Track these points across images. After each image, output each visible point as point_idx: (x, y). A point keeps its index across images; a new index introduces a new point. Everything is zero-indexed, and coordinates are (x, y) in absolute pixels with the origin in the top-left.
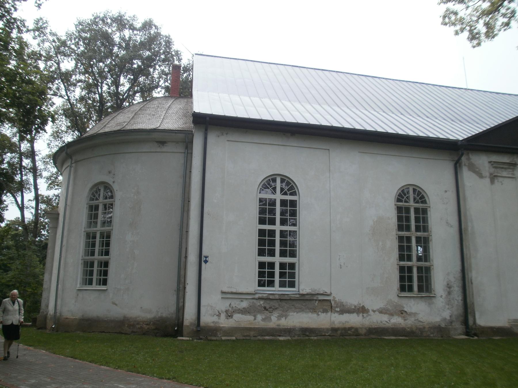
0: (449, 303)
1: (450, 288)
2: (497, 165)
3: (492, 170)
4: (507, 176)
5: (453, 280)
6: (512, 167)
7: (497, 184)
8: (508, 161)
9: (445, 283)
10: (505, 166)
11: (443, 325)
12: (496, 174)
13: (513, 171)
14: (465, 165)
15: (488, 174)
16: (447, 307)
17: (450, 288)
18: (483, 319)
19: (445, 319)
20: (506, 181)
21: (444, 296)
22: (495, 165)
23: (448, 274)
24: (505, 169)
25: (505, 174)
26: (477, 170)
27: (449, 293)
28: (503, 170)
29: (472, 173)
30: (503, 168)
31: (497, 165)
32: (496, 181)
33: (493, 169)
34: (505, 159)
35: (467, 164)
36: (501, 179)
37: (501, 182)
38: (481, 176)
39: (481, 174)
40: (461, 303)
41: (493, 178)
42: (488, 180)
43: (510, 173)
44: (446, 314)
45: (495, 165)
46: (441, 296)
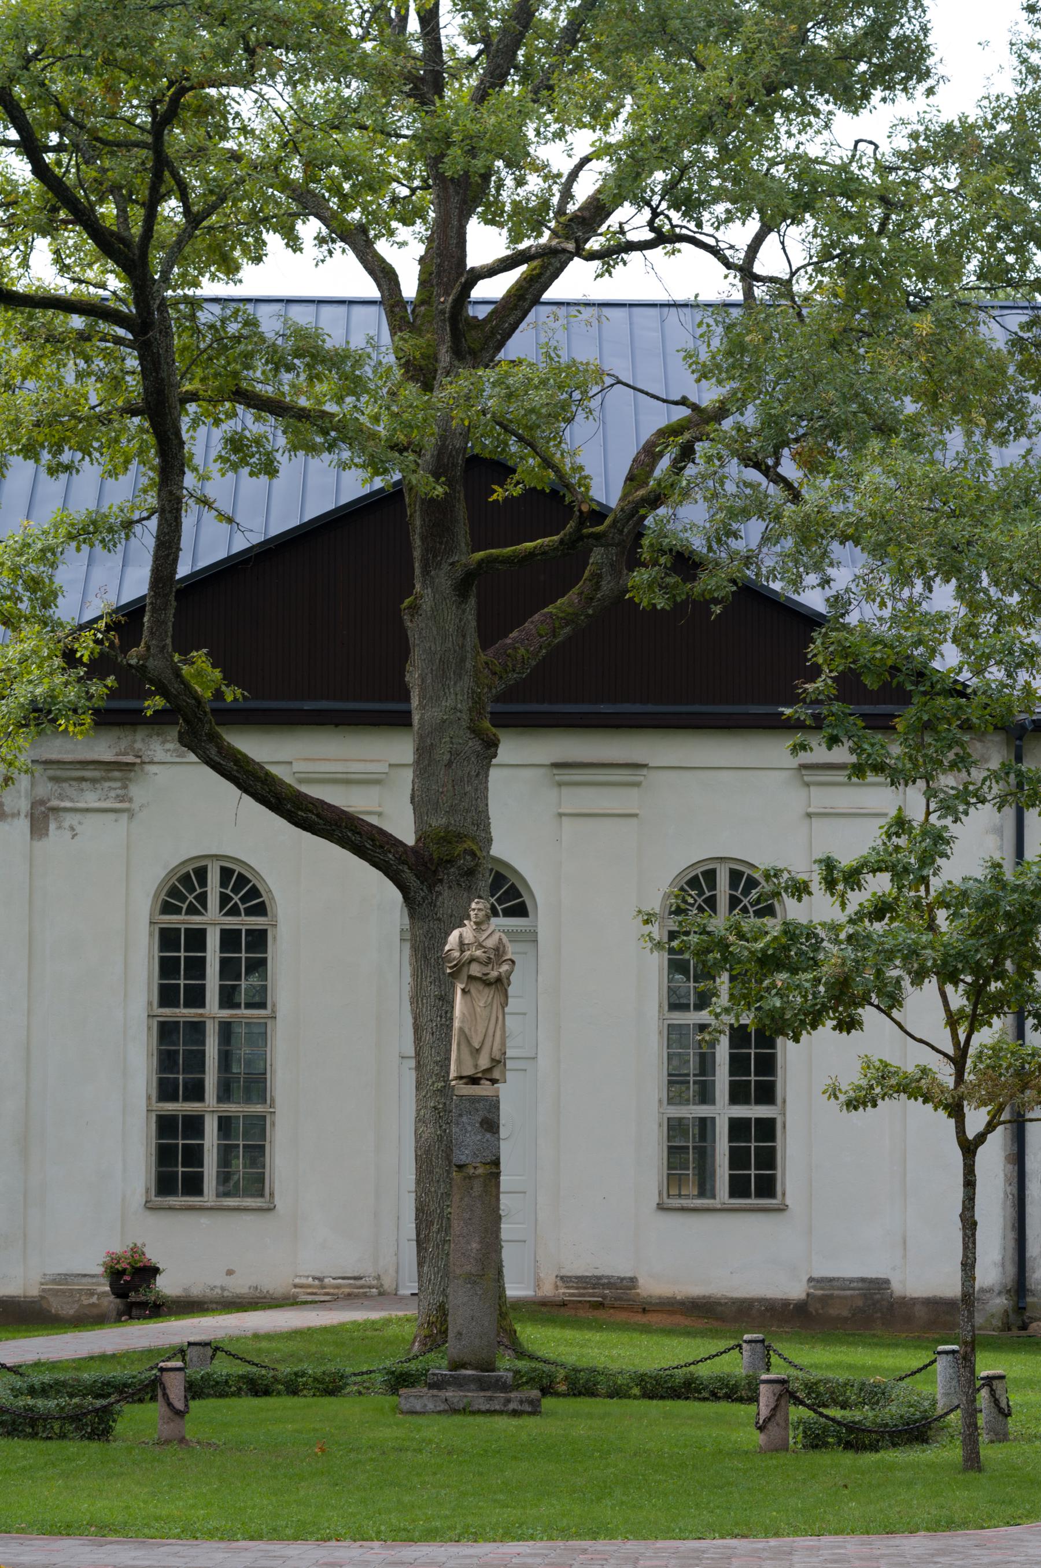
2: (59, 773)
3: (45, 789)
4: (97, 805)
6: (117, 774)
8: (108, 756)
10: (88, 774)
12: (54, 803)
13: (125, 787)
20: (90, 825)
22: (51, 773)
24: (94, 781)
25: (90, 798)
28: (84, 785)
30: (83, 779)
31: (59, 773)
32: (52, 826)
33: (50, 785)
36: (69, 819)
41: (41, 819)
42: (23, 825)
43: (113, 794)
45: (51, 773)
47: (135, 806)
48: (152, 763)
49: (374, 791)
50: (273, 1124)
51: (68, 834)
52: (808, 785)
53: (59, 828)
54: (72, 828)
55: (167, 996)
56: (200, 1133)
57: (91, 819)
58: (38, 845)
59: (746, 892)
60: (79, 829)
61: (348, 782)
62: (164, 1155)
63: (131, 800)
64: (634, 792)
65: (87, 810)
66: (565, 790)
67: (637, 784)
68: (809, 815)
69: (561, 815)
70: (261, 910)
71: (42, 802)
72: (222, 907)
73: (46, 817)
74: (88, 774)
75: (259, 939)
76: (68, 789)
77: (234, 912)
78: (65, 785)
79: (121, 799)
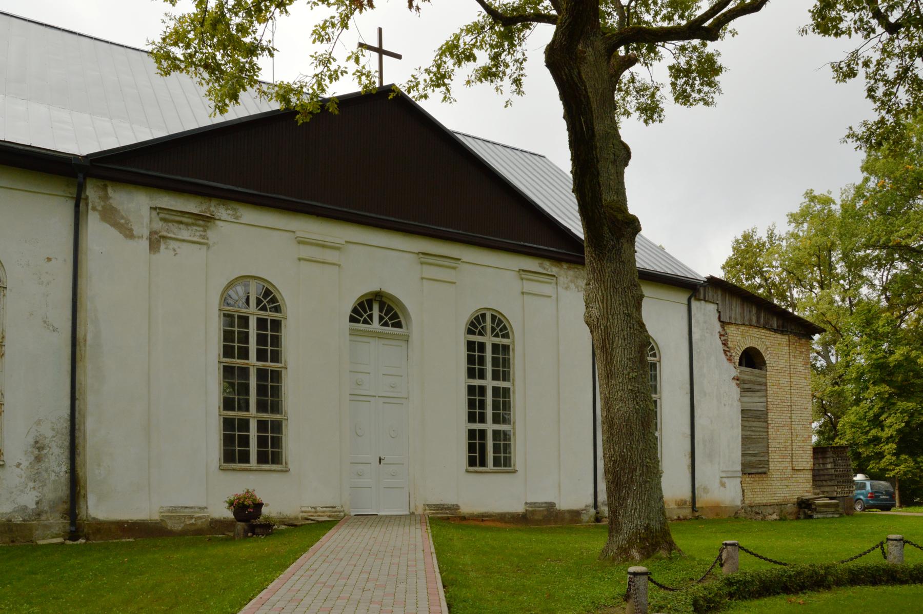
0: (36, 477)
1: (40, 449)
2: (167, 216)
3: (158, 225)
4: (190, 238)
5: (50, 434)
6: (201, 222)
7: (165, 252)
9: (32, 441)
10: (185, 220)
11: (18, 519)
12: (165, 234)
13: (205, 231)
14: (94, 209)
15: (146, 233)
16: (31, 484)
17: (40, 449)
18: (97, 508)
19: (25, 508)
20: (185, 248)
21: (25, 464)
23: (39, 422)
24: (187, 224)
25: (185, 234)
26: (123, 221)
27: (38, 459)
28: (181, 226)
29: (108, 226)
30: (181, 223)
31: (167, 216)
32: (163, 247)
33: (161, 223)
34: (192, 205)
35: (99, 208)
36: (173, 244)
37: (174, 250)
38: (129, 234)
39: (131, 230)
40: (64, 477)
41: (156, 241)
42: (145, 244)
43: (198, 234)
44: (29, 500)
46: (19, 465)
47: (210, 242)
48: (219, 220)
49: (336, 253)
50: (286, 426)
51: (172, 253)
52: (522, 279)
53: (167, 248)
54: (174, 250)
55: (228, 352)
56: (247, 429)
57: (185, 246)
58: (155, 257)
59: (498, 325)
60: (178, 251)
61: (323, 246)
62: (228, 440)
63: (208, 239)
64: (453, 271)
65: (184, 241)
66: (424, 266)
67: (454, 268)
68: (523, 293)
69: (422, 278)
70: (277, 309)
71: (156, 233)
72: (258, 305)
73: (159, 241)
74: (185, 220)
75: (277, 325)
76: (173, 227)
77: (264, 309)
78: (170, 224)
79: (204, 237)
